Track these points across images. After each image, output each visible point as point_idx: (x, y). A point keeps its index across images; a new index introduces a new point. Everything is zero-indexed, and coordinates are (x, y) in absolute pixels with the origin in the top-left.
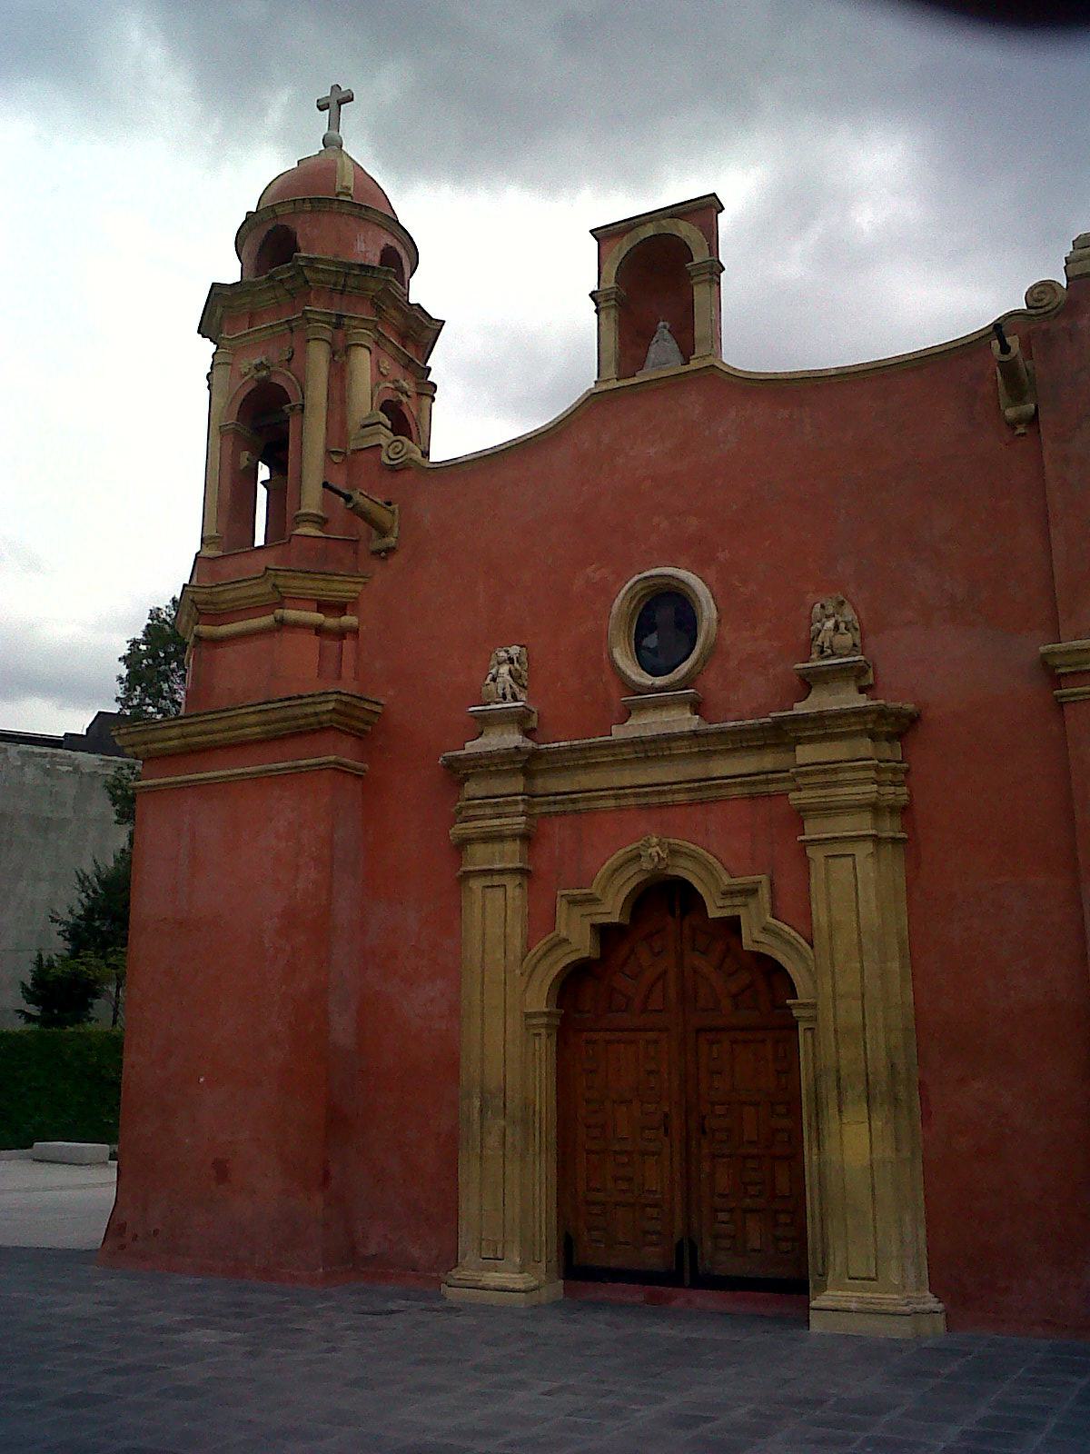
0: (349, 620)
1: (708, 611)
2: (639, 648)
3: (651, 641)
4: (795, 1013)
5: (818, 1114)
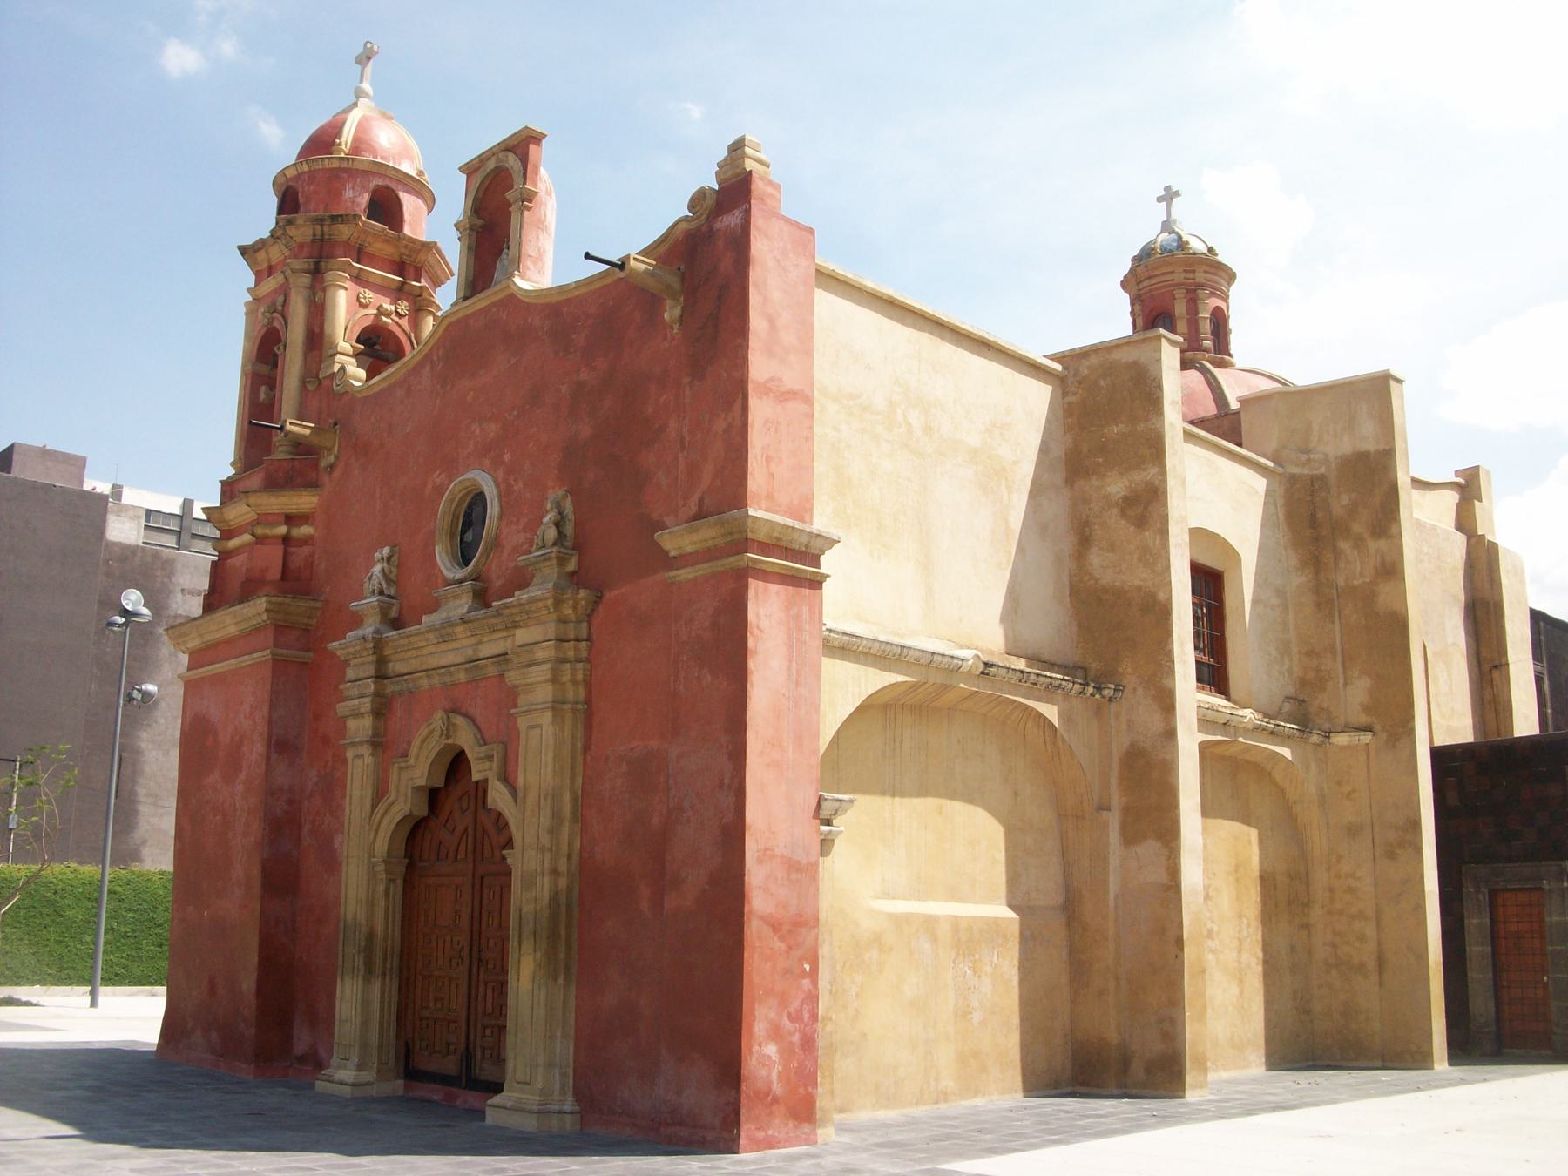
0: (305, 530)
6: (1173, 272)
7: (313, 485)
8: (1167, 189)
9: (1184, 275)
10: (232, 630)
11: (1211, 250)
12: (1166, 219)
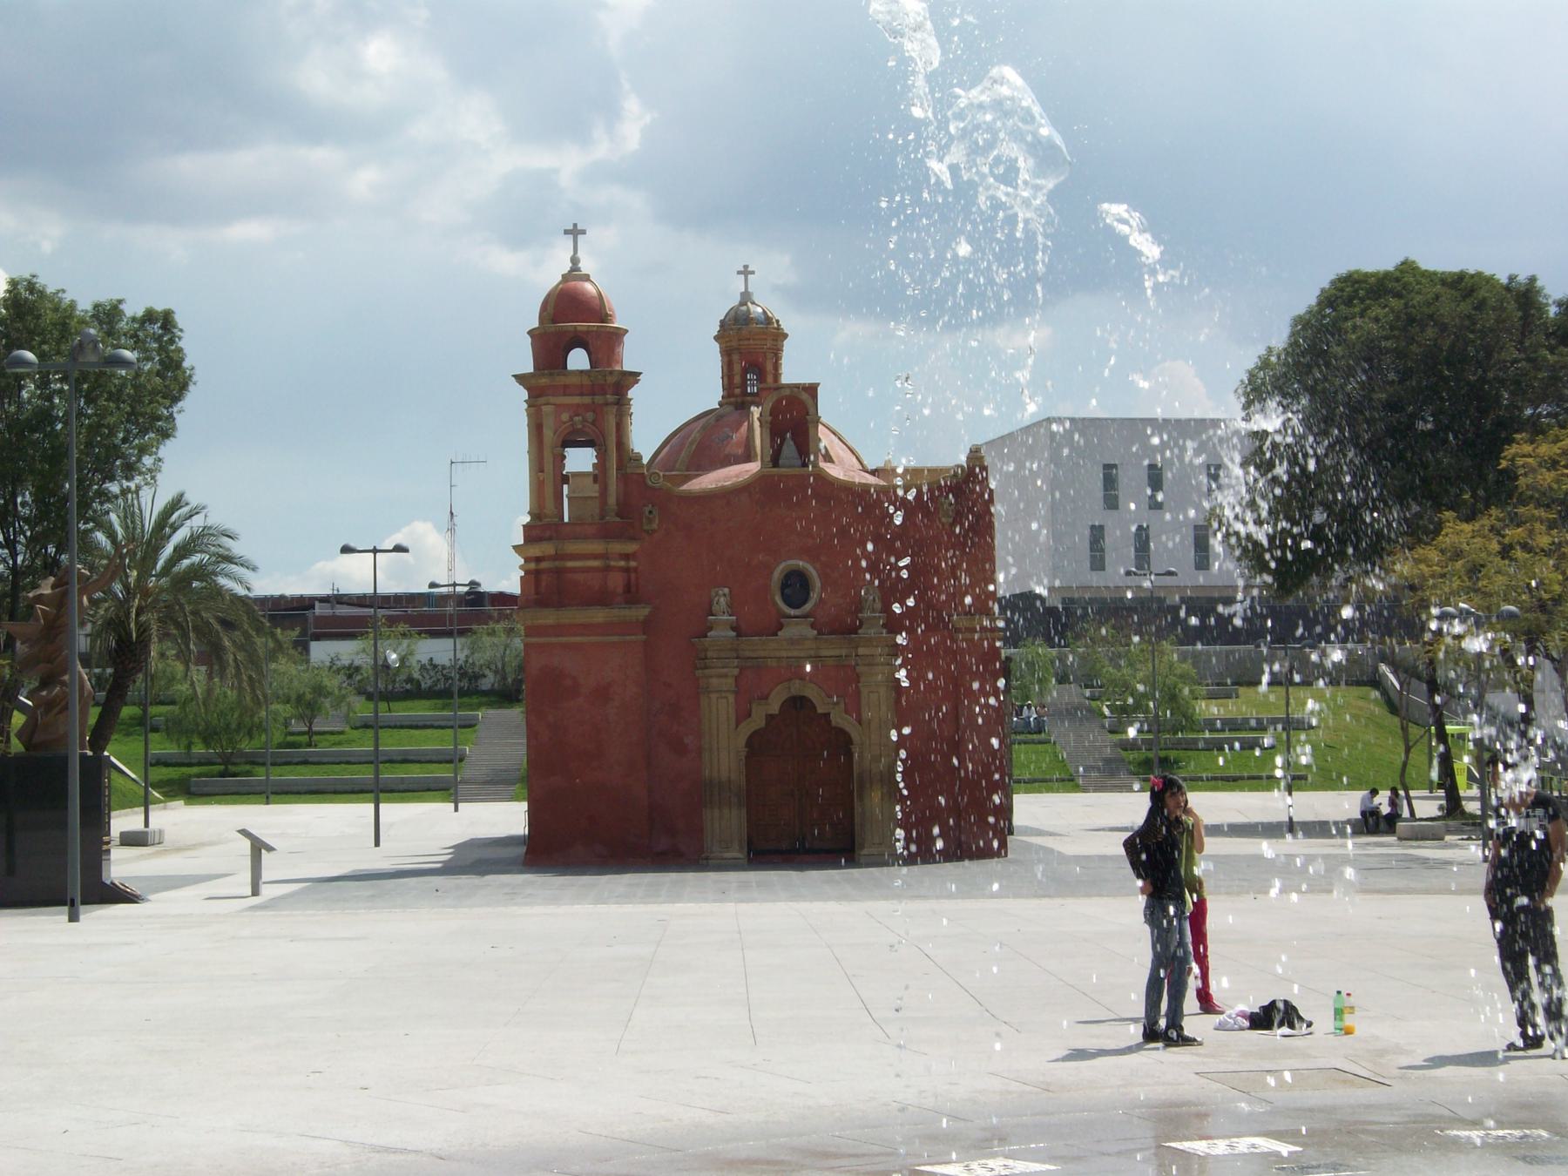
1: (818, 584)
2: (782, 594)
3: (787, 591)
5: (862, 787)
7: (633, 539)
8: (746, 267)
10: (600, 620)
11: (778, 321)
12: (743, 290)
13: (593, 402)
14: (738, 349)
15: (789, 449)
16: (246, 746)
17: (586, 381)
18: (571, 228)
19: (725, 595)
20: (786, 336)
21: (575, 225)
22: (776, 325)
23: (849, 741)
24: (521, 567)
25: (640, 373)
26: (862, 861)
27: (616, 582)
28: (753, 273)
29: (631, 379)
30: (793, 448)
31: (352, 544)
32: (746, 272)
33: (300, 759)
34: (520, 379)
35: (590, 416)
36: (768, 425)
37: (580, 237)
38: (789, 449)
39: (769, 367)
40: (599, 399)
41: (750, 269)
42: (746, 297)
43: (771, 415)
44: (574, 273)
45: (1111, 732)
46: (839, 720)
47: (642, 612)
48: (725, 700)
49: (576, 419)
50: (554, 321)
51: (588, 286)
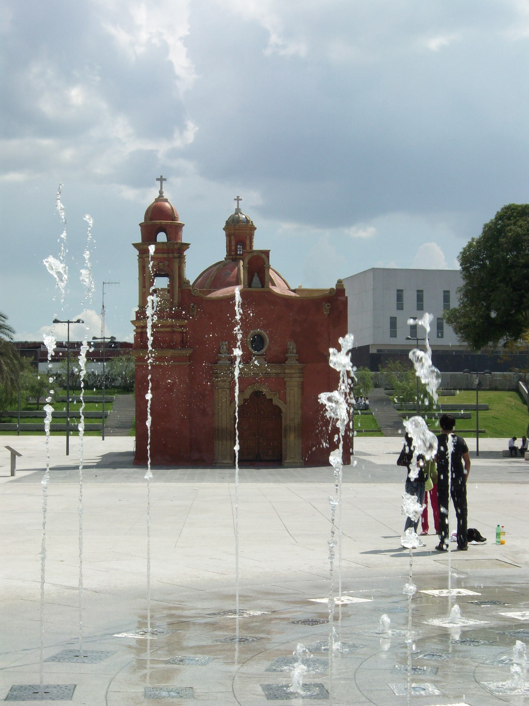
1: (268, 340)
4: (282, 416)
6: (246, 230)
8: (238, 197)
9: (249, 231)
11: (252, 222)
12: (237, 208)
13: (168, 257)
14: (234, 234)
15: (256, 280)
16: (9, 409)
17: (165, 247)
18: (160, 177)
19: (226, 345)
20: (255, 229)
21: (161, 176)
22: (251, 224)
23: (280, 411)
24: (134, 331)
25: (189, 244)
26: (285, 465)
27: (177, 338)
28: (241, 200)
29: (185, 246)
30: (258, 279)
31: (59, 319)
32: (238, 199)
33: (34, 415)
34: (136, 245)
35: (167, 263)
36: (247, 269)
37: (163, 182)
38: (256, 280)
39: (248, 242)
40: (171, 255)
41: (240, 198)
42: (238, 211)
43: (248, 264)
44: (161, 198)
45: (398, 410)
46: (276, 402)
47: (188, 352)
48: (225, 392)
49: (160, 264)
50: (151, 219)
51: (167, 204)
